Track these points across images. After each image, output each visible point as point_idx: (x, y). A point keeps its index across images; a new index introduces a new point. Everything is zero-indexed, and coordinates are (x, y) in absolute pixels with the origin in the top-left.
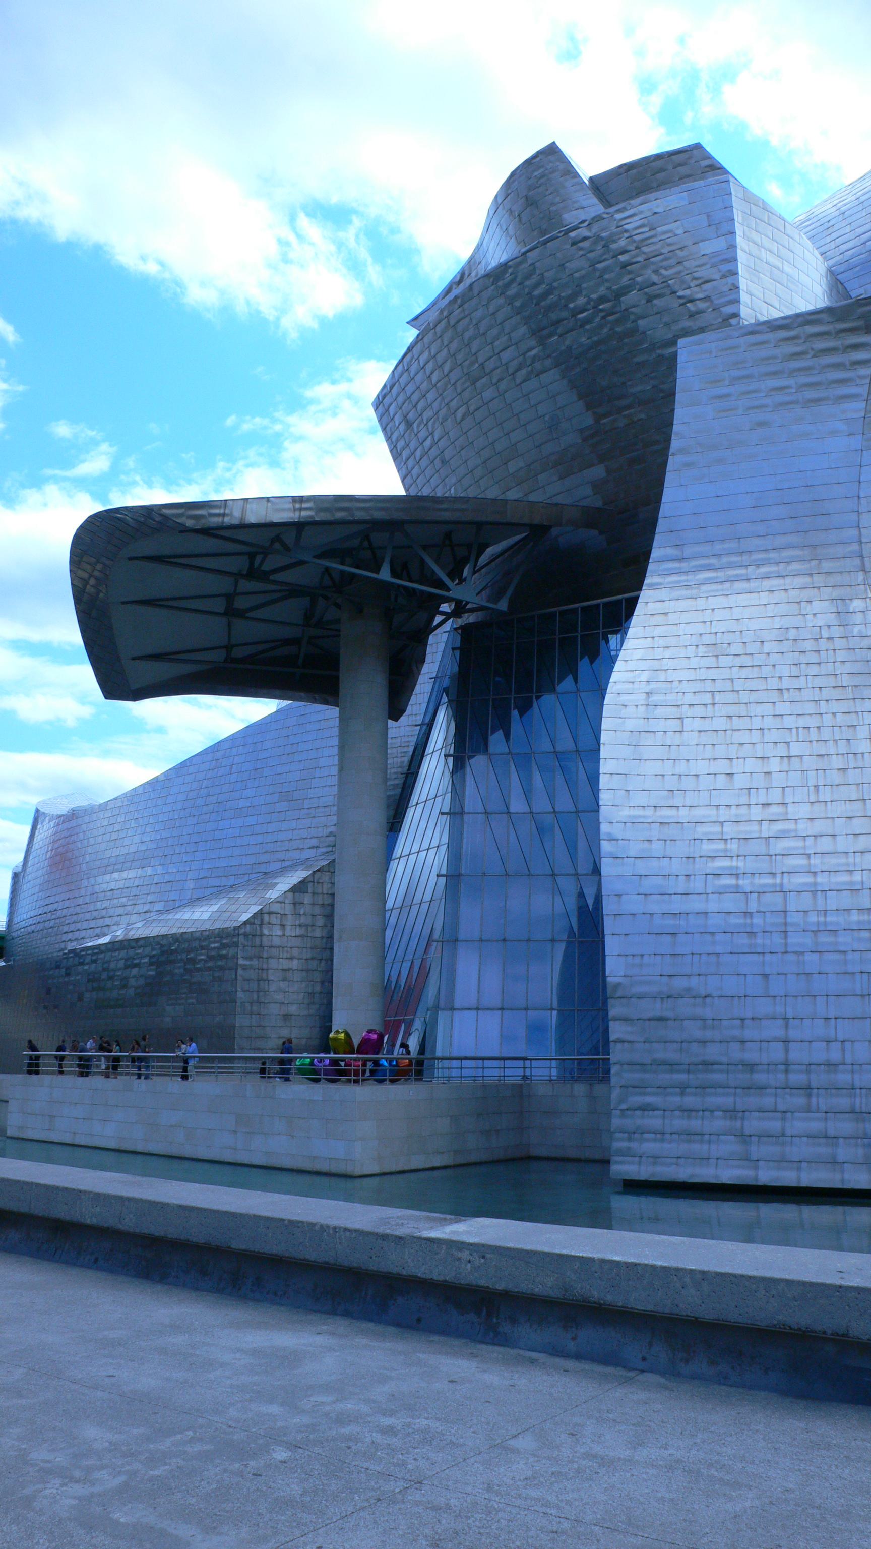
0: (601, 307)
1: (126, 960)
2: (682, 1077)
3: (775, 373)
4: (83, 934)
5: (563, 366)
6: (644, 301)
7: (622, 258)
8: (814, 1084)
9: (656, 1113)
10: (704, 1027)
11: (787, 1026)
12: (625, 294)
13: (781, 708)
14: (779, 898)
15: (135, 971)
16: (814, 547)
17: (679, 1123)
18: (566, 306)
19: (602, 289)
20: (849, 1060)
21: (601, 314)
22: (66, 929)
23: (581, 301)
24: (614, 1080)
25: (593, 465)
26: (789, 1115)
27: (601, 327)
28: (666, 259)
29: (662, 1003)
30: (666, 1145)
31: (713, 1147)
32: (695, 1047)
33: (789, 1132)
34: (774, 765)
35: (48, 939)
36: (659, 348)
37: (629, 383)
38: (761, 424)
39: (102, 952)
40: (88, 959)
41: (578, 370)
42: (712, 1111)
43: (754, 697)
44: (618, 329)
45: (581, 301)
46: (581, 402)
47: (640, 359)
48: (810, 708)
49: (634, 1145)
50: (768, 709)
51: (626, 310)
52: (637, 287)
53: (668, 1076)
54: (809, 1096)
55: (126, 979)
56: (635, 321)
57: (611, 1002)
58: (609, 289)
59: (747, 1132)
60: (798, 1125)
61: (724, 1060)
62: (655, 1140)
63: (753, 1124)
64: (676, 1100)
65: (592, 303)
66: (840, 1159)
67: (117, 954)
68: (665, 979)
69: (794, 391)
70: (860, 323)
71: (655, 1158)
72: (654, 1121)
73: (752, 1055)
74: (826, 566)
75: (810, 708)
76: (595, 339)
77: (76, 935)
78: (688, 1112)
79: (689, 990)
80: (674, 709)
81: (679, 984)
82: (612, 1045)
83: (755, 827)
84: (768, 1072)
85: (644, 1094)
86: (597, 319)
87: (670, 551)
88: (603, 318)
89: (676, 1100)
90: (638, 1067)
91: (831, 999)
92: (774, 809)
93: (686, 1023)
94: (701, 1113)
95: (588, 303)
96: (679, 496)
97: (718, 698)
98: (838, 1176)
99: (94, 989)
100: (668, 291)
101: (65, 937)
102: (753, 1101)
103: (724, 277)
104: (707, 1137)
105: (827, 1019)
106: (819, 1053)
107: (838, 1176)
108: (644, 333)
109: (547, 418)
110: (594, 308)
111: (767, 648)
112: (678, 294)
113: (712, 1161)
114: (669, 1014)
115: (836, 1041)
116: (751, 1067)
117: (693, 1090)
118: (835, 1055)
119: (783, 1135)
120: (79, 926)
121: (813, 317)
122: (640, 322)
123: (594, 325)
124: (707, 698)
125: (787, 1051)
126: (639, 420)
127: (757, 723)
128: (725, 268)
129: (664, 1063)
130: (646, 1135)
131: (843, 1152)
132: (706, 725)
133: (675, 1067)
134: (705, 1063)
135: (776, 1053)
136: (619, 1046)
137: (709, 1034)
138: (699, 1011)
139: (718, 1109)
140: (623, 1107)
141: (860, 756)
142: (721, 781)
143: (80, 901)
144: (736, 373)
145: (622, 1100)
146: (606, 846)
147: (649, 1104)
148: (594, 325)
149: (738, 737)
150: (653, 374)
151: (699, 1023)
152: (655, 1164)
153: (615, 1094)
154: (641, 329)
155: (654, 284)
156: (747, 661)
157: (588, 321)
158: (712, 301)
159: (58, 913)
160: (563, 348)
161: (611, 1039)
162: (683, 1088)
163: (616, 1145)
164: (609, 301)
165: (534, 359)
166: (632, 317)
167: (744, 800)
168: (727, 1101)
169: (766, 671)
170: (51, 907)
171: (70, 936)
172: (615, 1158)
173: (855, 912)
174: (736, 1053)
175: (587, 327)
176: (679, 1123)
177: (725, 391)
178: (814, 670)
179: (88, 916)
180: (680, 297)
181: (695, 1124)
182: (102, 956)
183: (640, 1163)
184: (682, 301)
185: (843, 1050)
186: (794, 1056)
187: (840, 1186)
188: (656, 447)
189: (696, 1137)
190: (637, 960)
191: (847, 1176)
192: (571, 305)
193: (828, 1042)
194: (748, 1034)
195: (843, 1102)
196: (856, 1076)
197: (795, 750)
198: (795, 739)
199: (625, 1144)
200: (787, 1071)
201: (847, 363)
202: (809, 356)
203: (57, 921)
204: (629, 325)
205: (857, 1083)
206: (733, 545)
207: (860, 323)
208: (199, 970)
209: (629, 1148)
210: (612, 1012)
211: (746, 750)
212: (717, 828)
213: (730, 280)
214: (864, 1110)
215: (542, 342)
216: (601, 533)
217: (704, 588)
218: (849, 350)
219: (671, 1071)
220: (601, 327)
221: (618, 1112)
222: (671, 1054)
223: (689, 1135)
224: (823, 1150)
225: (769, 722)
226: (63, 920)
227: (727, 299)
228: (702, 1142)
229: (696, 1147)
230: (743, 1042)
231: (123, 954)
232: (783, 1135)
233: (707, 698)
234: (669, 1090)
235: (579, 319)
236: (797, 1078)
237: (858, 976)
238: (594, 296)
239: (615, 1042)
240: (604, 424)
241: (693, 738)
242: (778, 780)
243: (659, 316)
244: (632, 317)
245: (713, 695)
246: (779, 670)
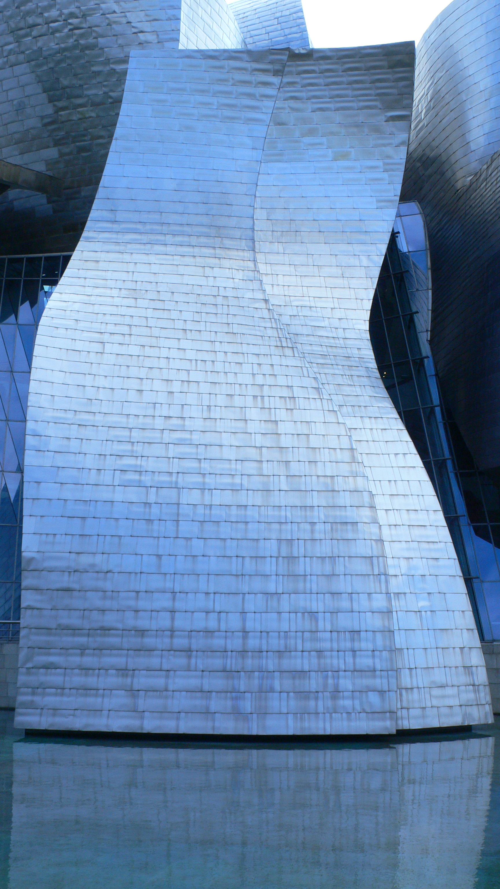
0: (70, 21)
2: (83, 640)
3: (203, 91)
5: (33, 63)
6: (105, 24)
8: (194, 647)
9: (58, 670)
10: (104, 598)
11: (174, 599)
12: (90, 15)
13: (184, 344)
14: (174, 492)
16: (219, 227)
17: (78, 680)
18: (41, 14)
19: (73, 6)
20: (223, 627)
21: (70, 27)
23: (54, 13)
24: (22, 642)
25: (48, 147)
26: (172, 673)
27: (68, 36)
29: (69, 576)
30: (65, 699)
31: (106, 700)
32: (95, 615)
33: (171, 687)
34: (176, 387)
36: (113, 63)
37: (85, 86)
41: (45, 68)
42: (107, 670)
43: (164, 333)
44: (82, 42)
45: (54, 13)
46: (45, 95)
47: (95, 69)
48: (207, 346)
49: (37, 699)
50: (173, 343)
51: (89, 27)
52: (101, 12)
53: (70, 639)
54: (190, 657)
56: (96, 38)
57: (24, 574)
58: (79, 8)
59: (136, 687)
60: (179, 681)
61: (120, 626)
62: (56, 695)
63: (142, 681)
64: (76, 660)
65: (63, 16)
66: (213, 709)
68: (73, 556)
69: (215, 108)
70: (269, 67)
71: (55, 710)
72: (55, 678)
73: (143, 623)
74: (227, 243)
75: (207, 346)
76: (63, 45)
78: (86, 670)
79: (93, 565)
80: (97, 335)
81: (85, 560)
82: (22, 611)
83: (158, 434)
84: (156, 636)
85: (49, 654)
86: (66, 30)
87: (106, 214)
88: (70, 30)
89: (76, 660)
90: (43, 631)
91: (212, 577)
92: (174, 421)
93: (89, 594)
94: (97, 671)
95: (60, 15)
96: (118, 173)
97: (134, 330)
98: (210, 724)
100: (124, 21)
102: (142, 661)
103: (169, 19)
104: (101, 692)
105: (207, 593)
106: (199, 622)
107: (210, 724)
108: (102, 49)
109: (15, 102)
110: (64, 20)
111: (176, 297)
112: (132, 24)
113: (105, 713)
114: (76, 586)
115: (214, 612)
116: (142, 632)
117: (91, 651)
118: (212, 624)
119: (166, 690)
122: (100, 39)
123: (62, 34)
124: (125, 330)
125: (173, 619)
126: (90, 117)
127: (164, 353)
128: (171, 12)
129: (67, 628)
130: (47, 690)
131: (215, 704)
132: (123, 350)
133: (77, 631)
134: (103, 629)
135: (164, 621)
136: (29, 612)
137: (108, 604)
138: (100, 584)
139: (113, 668)
140: (29, 665)
141: (244, 386)
142: (132, 396)
144: (172, 85)
145: (28, 659)
146: (30, 441)
147: (52, 663)
148: (62, 34)
149: (148, 363)
150: (105, 83)
151: (100, 594)
152: (54, 715)
153: (22, 655)
154: (100, 46)
155: (114, 12)
156: (159, 305)
158: (158, 35)
160: (35, 48)
161: (22, 606)
162: (83, 650)
163: (21, 698)
164: (77, 17)
165: (10, 52)
166: (94, 34)
167: (150, 412)
168: (120, 661)
169: (174, 315)
172: (17, 710)
173: (234, 508)
174: (130, 620)
175: (57, 35)
176: (78, 680)
177: (162, 97)
178: (212, 318)
180: (133, 27)
181: (91, 681)
183: (41, 715)
185: (219, 620)
186: (179, 623)
187: (211, 732)
188: (100, 141)
189: (92, 692)
190: (50, 538)
191: (217, 724)
192: (46, 15)
193: (207, 612)
194: (142, 604)
195: (217, 662)
196: (229, 641)
197: (194, 376)
198: (194, 368)
199: (29, 698)
200: (172, 637)
201: (257, 95)
202: (230, 84)
204: (91, 40)
205: (229, 647)
206: (156, 217)
207: (269, 67)
209: (32, 702)
210: (25, 583)
211: (155, 373)
212: (126, 433)
214: (233, 670)
215: (18, 41)
216: (49, 202)
217: (129, 246)
218: (260, 85)
219: (74, 635)
220: (68, 36)
221: (24, 670)
222: (75, 621)
223: (86, 690)
224: (199, 702)
225: (174, 353)
227: (171, 36)
228: (96, 696)
229: (91, 700)
230: (137, 611)
232: (166, 690)
233: (125, 330)
234: (71, 651)
235: (51, 27)
236: (180, 642)
237: (234, 559)
238: (66, 11)
239: (26, 608)
240: (61, 115)
241: (112, 359)
242: (178, 398)
243: (115, 38)
244: (94, 34)
245: (130, 328)
246: (186, 316)
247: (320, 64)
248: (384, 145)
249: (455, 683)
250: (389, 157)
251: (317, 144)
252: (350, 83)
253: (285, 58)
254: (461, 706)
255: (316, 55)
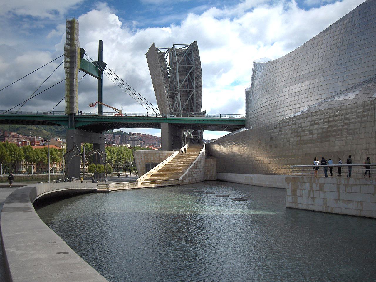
1: (311, 122)
4: (286, 112)
15: (316, 126)
22: (277, 111)
35: (269, 117)
39: (298, 119)
40: (291, 123)
55: (312, 130)
67: (306, 119)
77: (283, 113)
99: (295, 136)
101: (277, 115)
120: (284, 109)
143: (283, 98)
159: (273, 105)
170: (268, 103)
171: (280, 114)
179: (288, 104)
182: (298, 121)
203: (273, 108)
208: (352, 123)
226: (275, 107)
231: (309, 119)
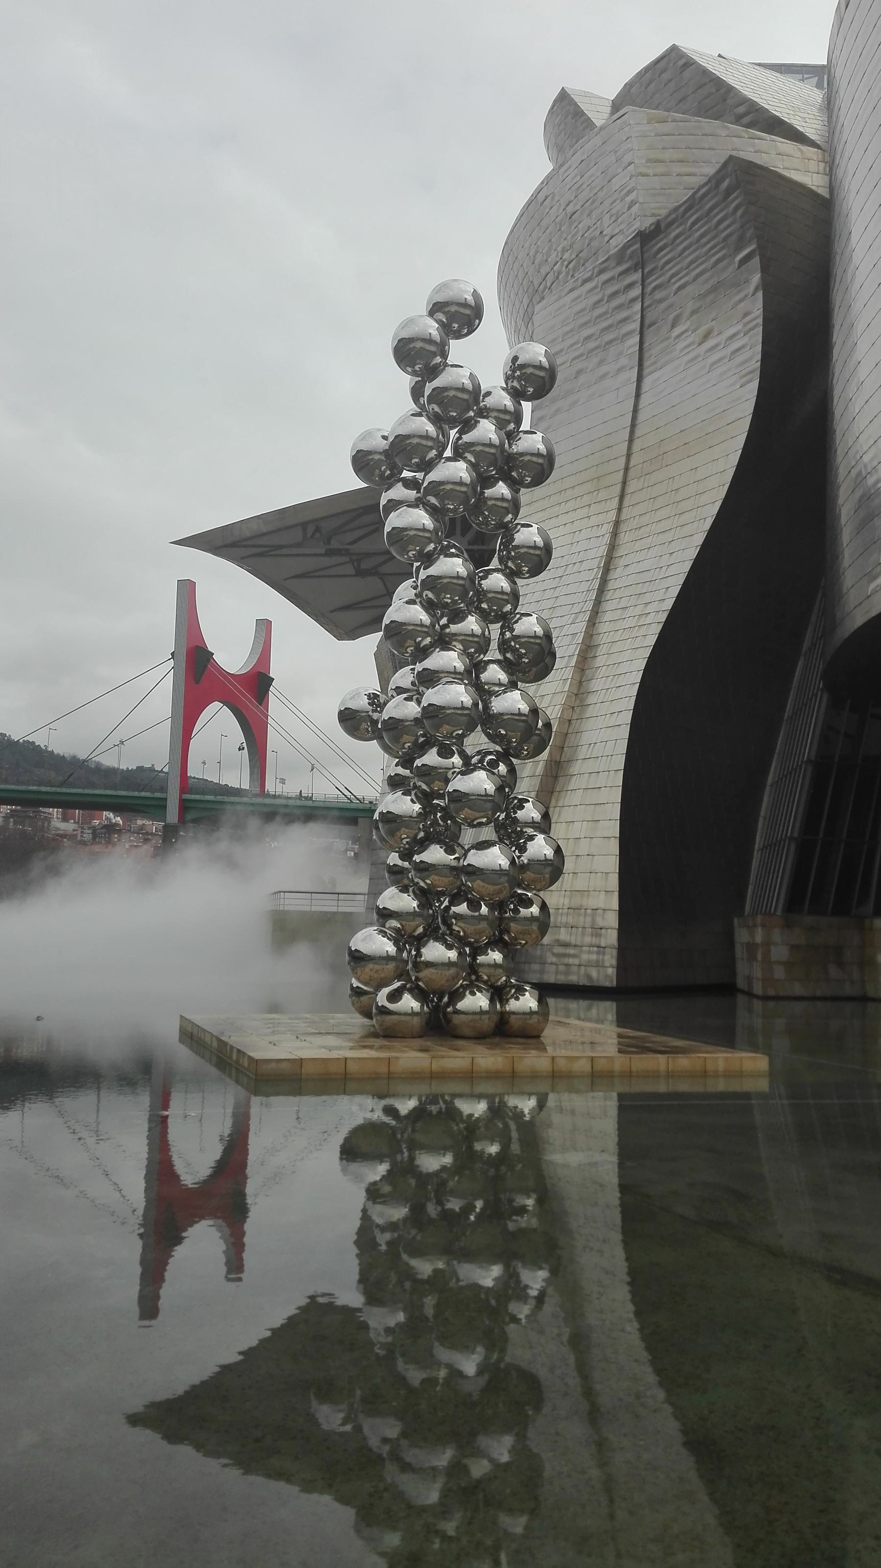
3: (585, 324)
7: (570, 209)
21: (566, 263)
23: (554, 254)
28: (593, 202)
38: (579, 372)
88: (567, 266)
121: (603, 266)
123: (564, 274)
128: (629, 199)
157: (559, 273)
166: (582, 262)
175: (560, 277)
184: (606, 239)
213: (635, 209)
238: (559, 249)
247: (670, 233)
248: (741, 301)
249: (579, 943)
250: (746, 315)
251: (682, 333)
252: (698, 241)
253: (638, 246)
254: (580, 965)
255: (663, 226)
